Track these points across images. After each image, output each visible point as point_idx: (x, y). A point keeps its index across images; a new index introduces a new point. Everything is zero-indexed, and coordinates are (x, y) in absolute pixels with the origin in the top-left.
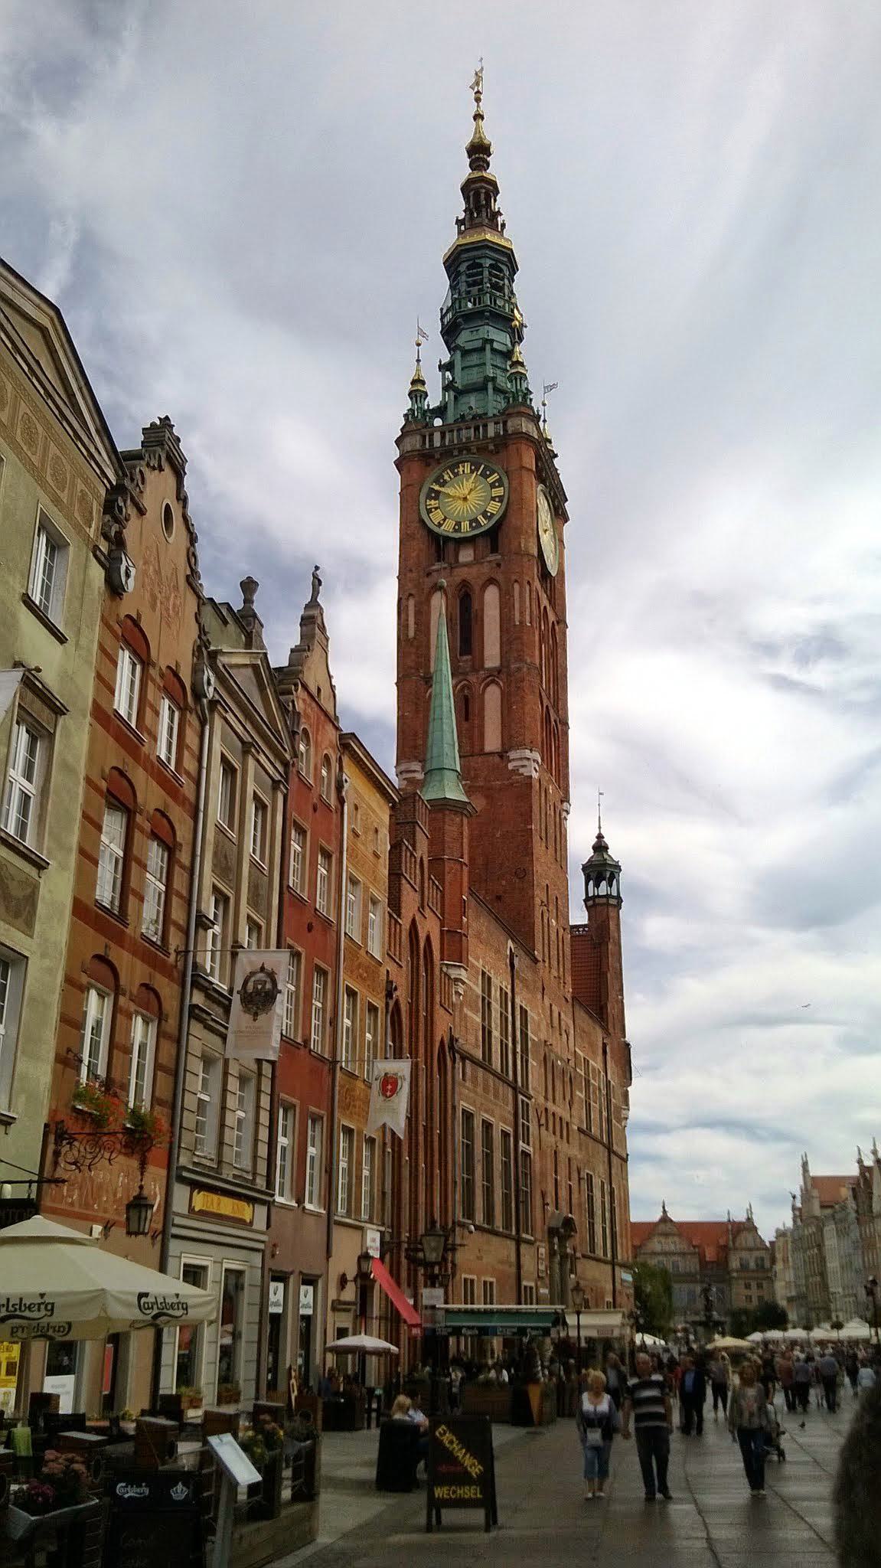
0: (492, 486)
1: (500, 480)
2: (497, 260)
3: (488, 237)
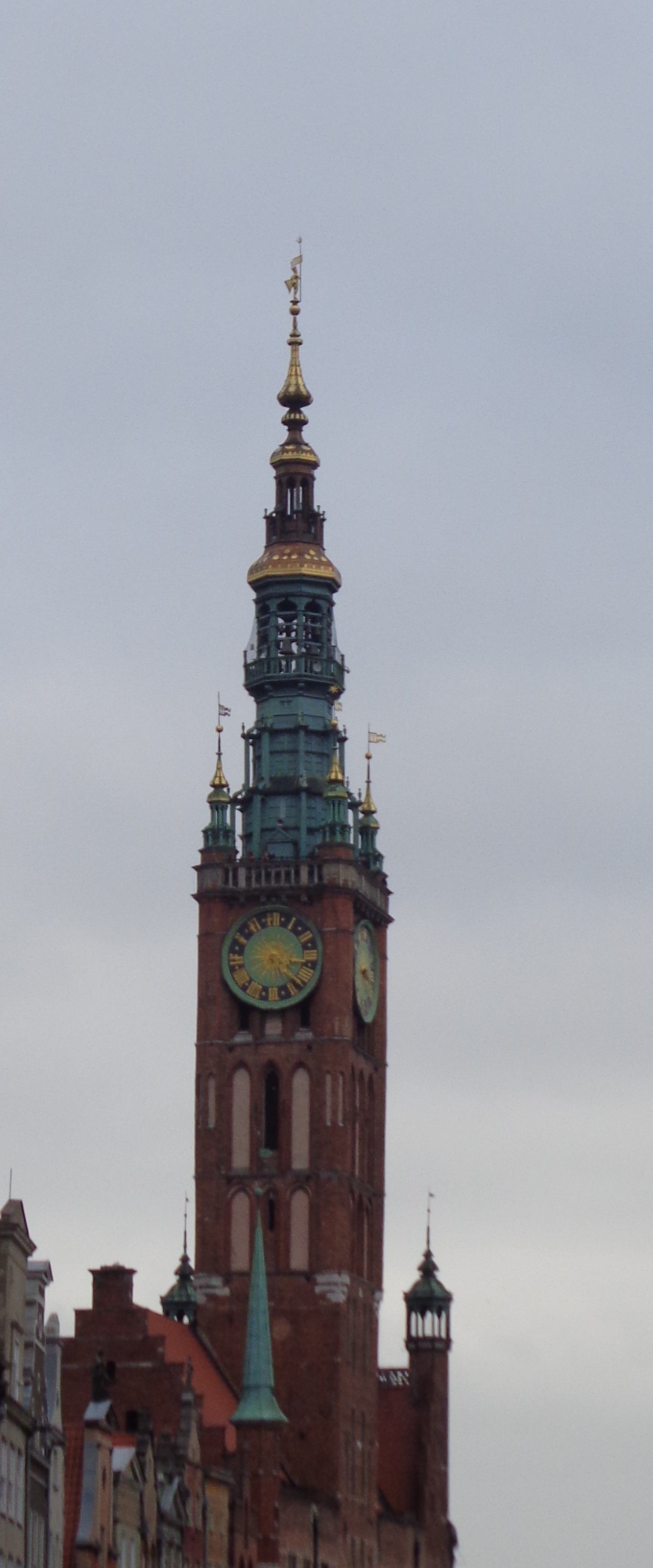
0: (305, 947)
1: (313, 941)
2: (315, 597)
3: (306, 570)
